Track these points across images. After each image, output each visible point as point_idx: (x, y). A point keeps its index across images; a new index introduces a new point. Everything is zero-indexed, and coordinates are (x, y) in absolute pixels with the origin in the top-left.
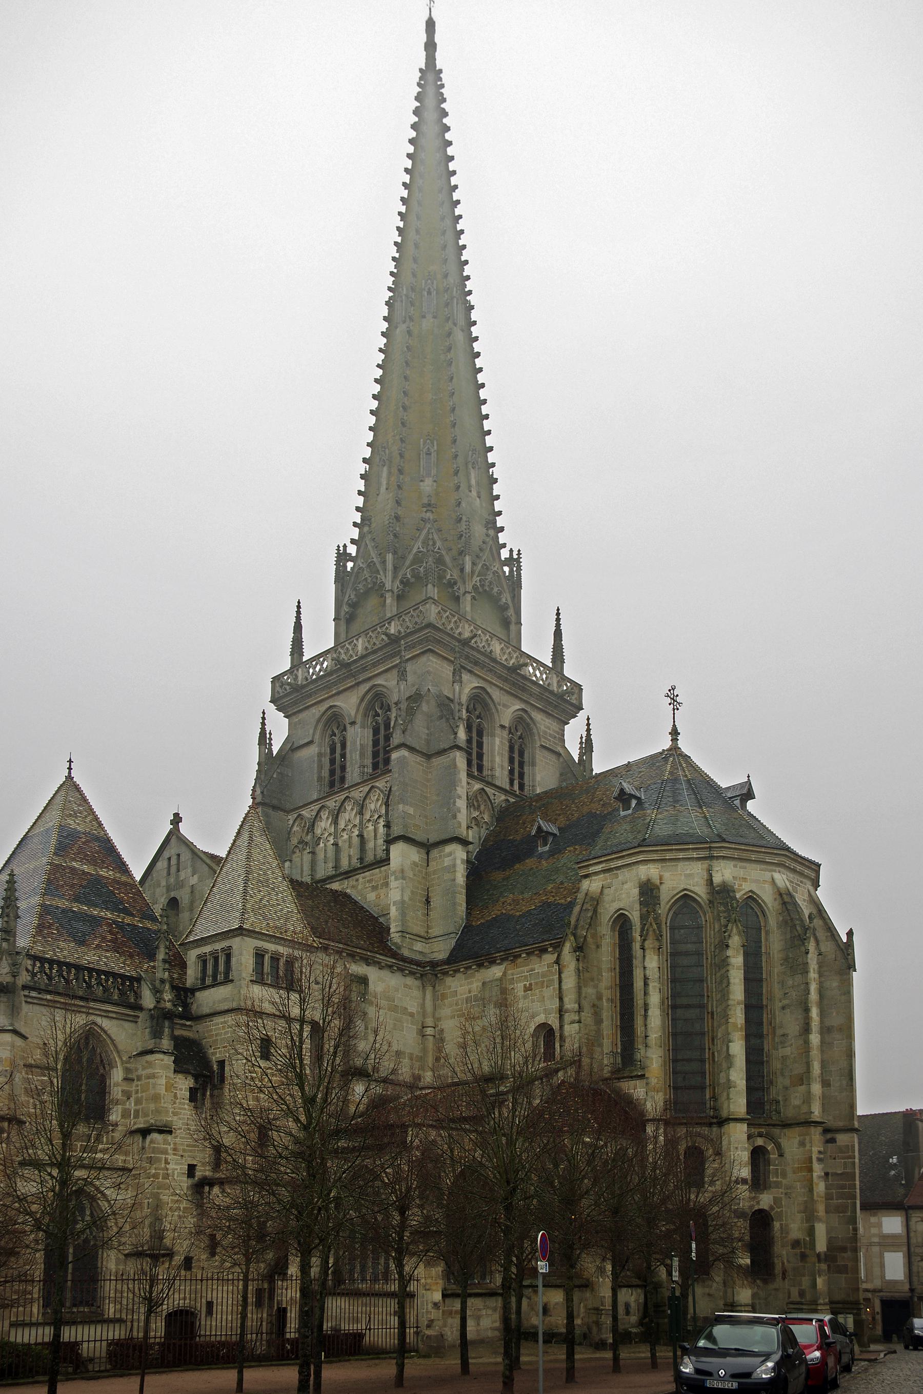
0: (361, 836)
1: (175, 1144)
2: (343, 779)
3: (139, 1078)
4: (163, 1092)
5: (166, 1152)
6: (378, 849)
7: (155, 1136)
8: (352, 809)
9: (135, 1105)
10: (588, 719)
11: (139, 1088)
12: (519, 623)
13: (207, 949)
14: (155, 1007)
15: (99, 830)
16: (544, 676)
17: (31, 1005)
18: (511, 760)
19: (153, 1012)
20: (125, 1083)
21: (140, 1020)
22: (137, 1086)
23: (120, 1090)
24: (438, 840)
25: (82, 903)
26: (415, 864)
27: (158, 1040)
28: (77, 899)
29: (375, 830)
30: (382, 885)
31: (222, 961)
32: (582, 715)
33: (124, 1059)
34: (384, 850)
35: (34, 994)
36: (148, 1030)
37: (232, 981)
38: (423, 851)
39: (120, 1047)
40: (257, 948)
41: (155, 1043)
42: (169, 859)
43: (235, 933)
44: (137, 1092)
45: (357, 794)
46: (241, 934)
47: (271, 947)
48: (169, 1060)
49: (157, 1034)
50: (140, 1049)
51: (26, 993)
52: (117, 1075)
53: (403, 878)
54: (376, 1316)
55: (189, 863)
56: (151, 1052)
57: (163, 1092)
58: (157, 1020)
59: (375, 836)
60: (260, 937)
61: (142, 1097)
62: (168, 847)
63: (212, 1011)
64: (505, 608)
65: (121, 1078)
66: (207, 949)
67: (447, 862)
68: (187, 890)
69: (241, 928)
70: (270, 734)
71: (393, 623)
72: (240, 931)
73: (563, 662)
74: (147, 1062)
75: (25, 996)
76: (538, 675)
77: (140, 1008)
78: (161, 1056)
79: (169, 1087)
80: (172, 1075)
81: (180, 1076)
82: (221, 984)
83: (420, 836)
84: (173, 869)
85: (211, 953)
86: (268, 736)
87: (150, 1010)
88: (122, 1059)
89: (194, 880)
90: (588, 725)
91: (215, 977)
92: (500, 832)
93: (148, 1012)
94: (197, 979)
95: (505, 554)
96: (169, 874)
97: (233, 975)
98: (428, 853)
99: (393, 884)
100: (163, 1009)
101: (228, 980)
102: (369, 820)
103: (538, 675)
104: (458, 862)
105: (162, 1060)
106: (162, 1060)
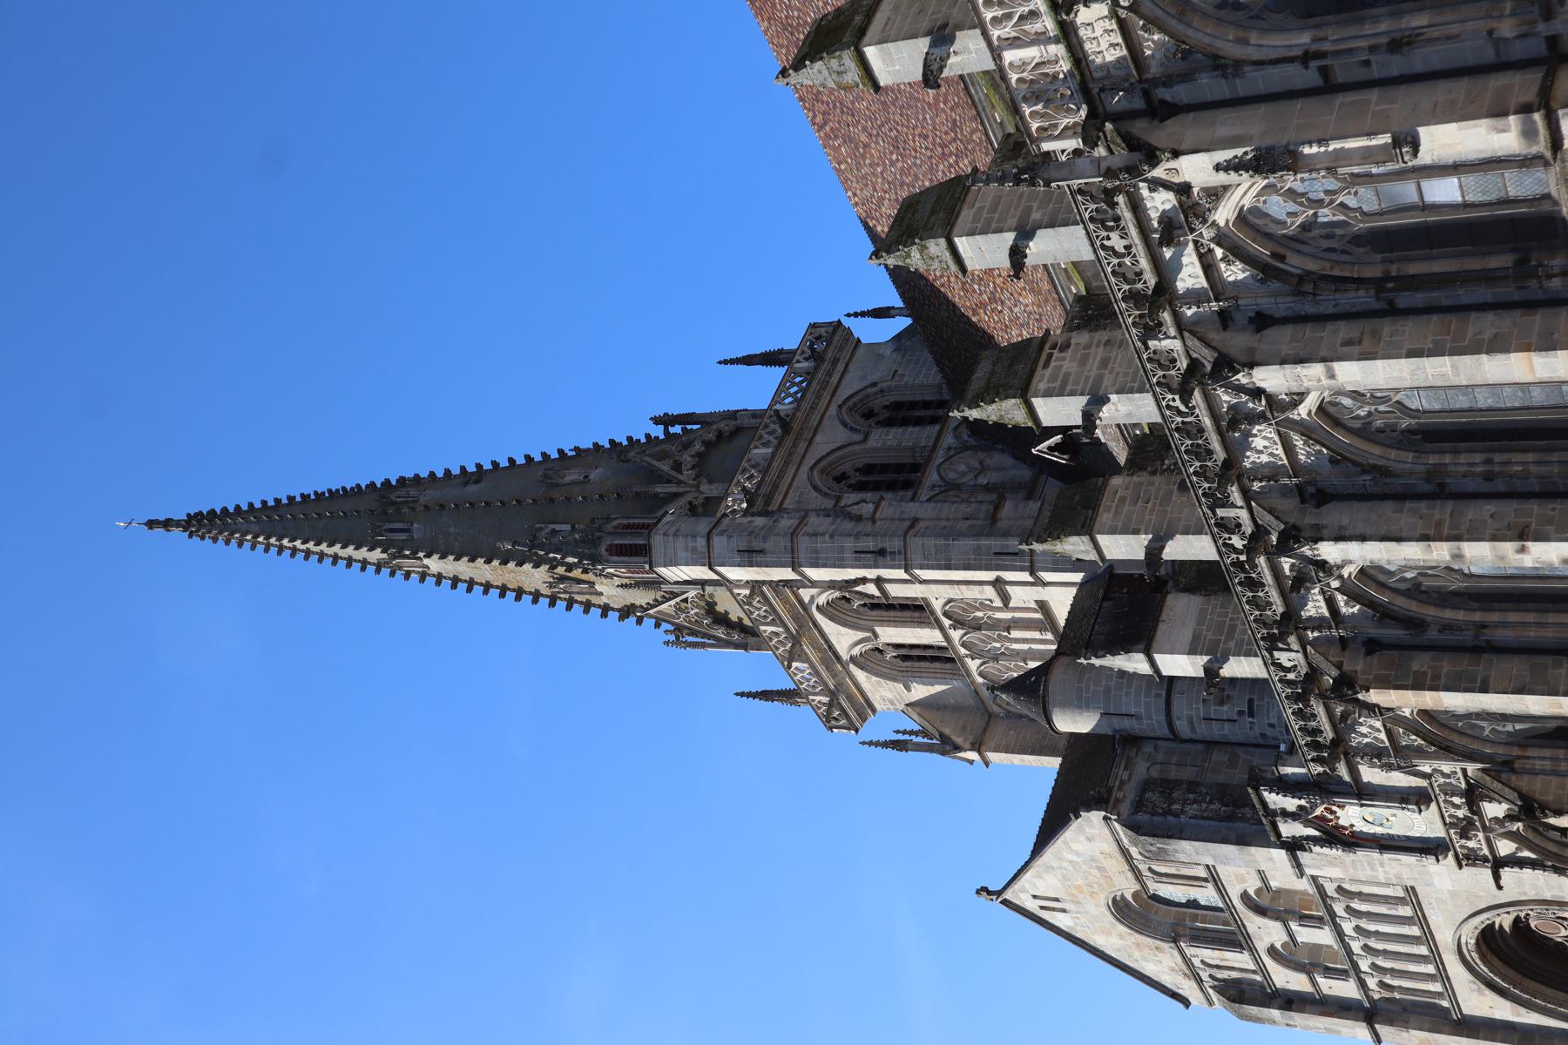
2: (940, 648)
10: (849, 315)
12: (732, 415)
16: (798, 379)
18: (905, 422)
32: (847, 322)
42: (1042, 908)
45: (956, 635)
64: (720, 434)
70: (898, 732)
71: (736, 591)
73: (781, 351)
76: (795, 389)
86: (900, 737)
90: (856, 315)
95: (658, 431)
103: (795, 389)
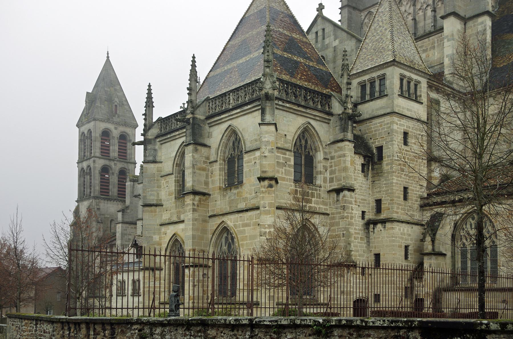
0: (414, 19)
1: (355, 198)
3: (332, 158)
4: (349, 165)
5: (351, 203)
6: (427, 26)
7: (346, 193)
8: (407, 4)
9: (330, 174)
11: (333, 164)
13: (366, 77)
14: (343, 113)
15: (288, 11)
17: (278, 110)
19: (341, 116)
20: (324, 161)
21: (331, 122)
22: (331, 163)
23: (322, 165)
24: (472, 15)
25: (288, 52)
26: (458, 31)
27: (346, 133)
28: (285, 50)
29: (425, 15)
30: (431, 48)
31: (377, 84)
33: (324, 146)
34: (432, 26)
35: (280, 103)
36: (338, 128)
37: (387, 95)
38: (463, 23)
39: (322, 139)
40: (401, 75)
41: (344, 135)
42: (317, 33)
43: (389, 64)
44: (331, 167)
46: (394, 65)
47: (407, 74)
48: (351, 146)
49: (344, 130)
50: (332, 140)
51: (276, 102)
52: (320, 156)
53: (453, 40)
54: (488, 304)
55: (332, 33)
56: (342, 141)
57: (349, 165)
58: (345, 121)
59: (425, 18)
60: (402, 67)
61: (335, 169)
62: (315, 25)
63: (371, 116)
65: (322, 158)
66: (366, 77)
67: (480, 28)
68: (331, 50)
69: (394, 60)
72: (394, 63)
74: (338, 147)
75: (276, 104)
77: (330, 114)
78: (347, 143)
79: (353, 163)
80: (353, 155)
81: (357, 156)
82: (378, 98)
83: (462, 14)
84: (320, 38)
85: (369, 80)
87: (339, 115)
88: (323, 146)
89: (336, 43)
91: (372, 94)
92: (504, 11)
93: (337, 116)
94: (357, 97)
96: (317, 42)
97: (388, 91)
98: (465, 24)
99: (446, 44)
100: (348, 113)
101: (382, 95)
102: (420, 9)
104: (488, 28)
105: (348, 146)
106: (348, 146)
